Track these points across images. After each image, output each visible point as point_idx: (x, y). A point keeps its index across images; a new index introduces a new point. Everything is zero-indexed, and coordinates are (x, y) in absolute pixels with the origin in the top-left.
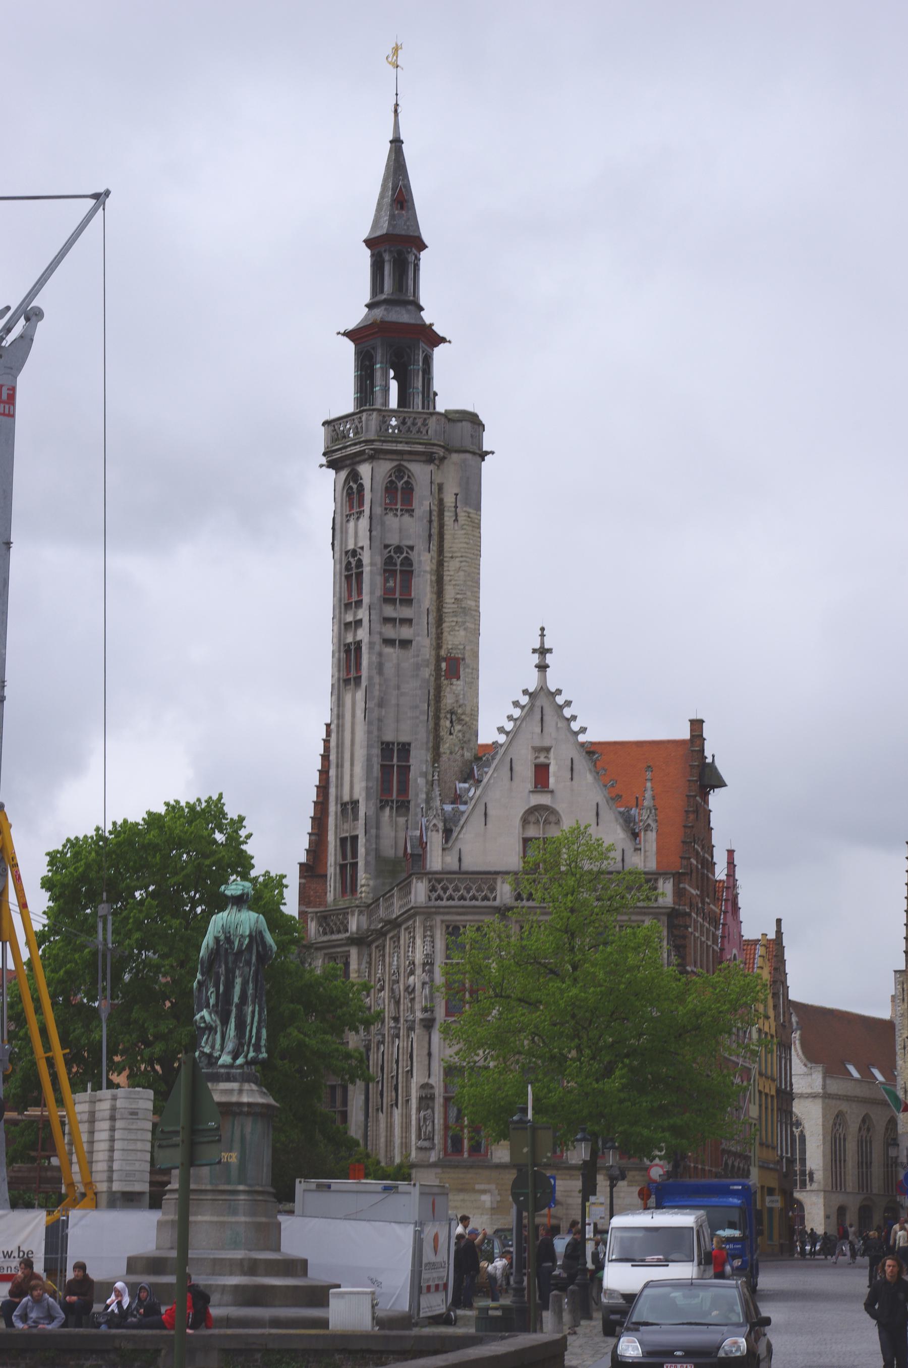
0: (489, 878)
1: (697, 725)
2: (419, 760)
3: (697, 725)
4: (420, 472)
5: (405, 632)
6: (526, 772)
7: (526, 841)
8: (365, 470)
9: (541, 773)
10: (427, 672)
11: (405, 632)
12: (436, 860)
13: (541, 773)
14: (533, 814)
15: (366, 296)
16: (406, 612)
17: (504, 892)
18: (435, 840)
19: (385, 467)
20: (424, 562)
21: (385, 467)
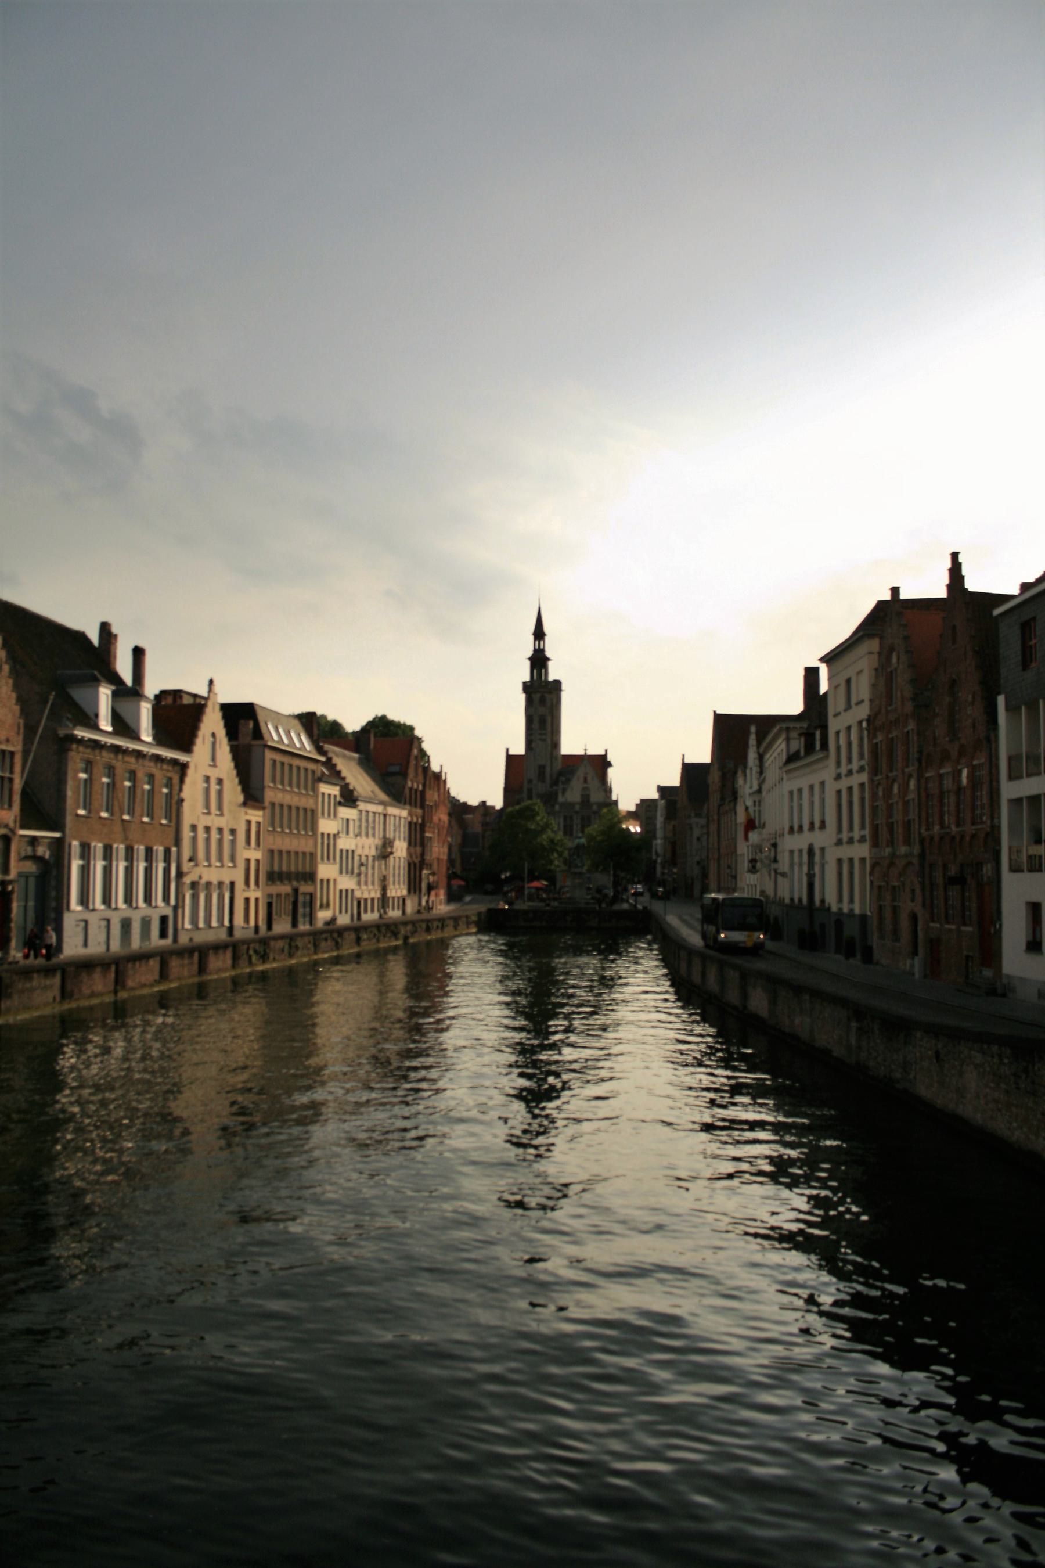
0: (572, 805)
1: (606, 751)
2: (548, 770)
3: (606, 751)
4: (548, 696)
5: (544, 737)
6: (582, 780)
7: (582, 796)
8: (533, 696)
9: (585, 780)
10: (549, 748)
11: (544, 737)
12: (561, 799)
13: (585, 780)
14: (585, 789)
15: (532, 649)
16: (544, 732)
17: (577, 807)
18: (560, 795)
19: (538, 695)
20: (549, 719)
21: (538, 695)
